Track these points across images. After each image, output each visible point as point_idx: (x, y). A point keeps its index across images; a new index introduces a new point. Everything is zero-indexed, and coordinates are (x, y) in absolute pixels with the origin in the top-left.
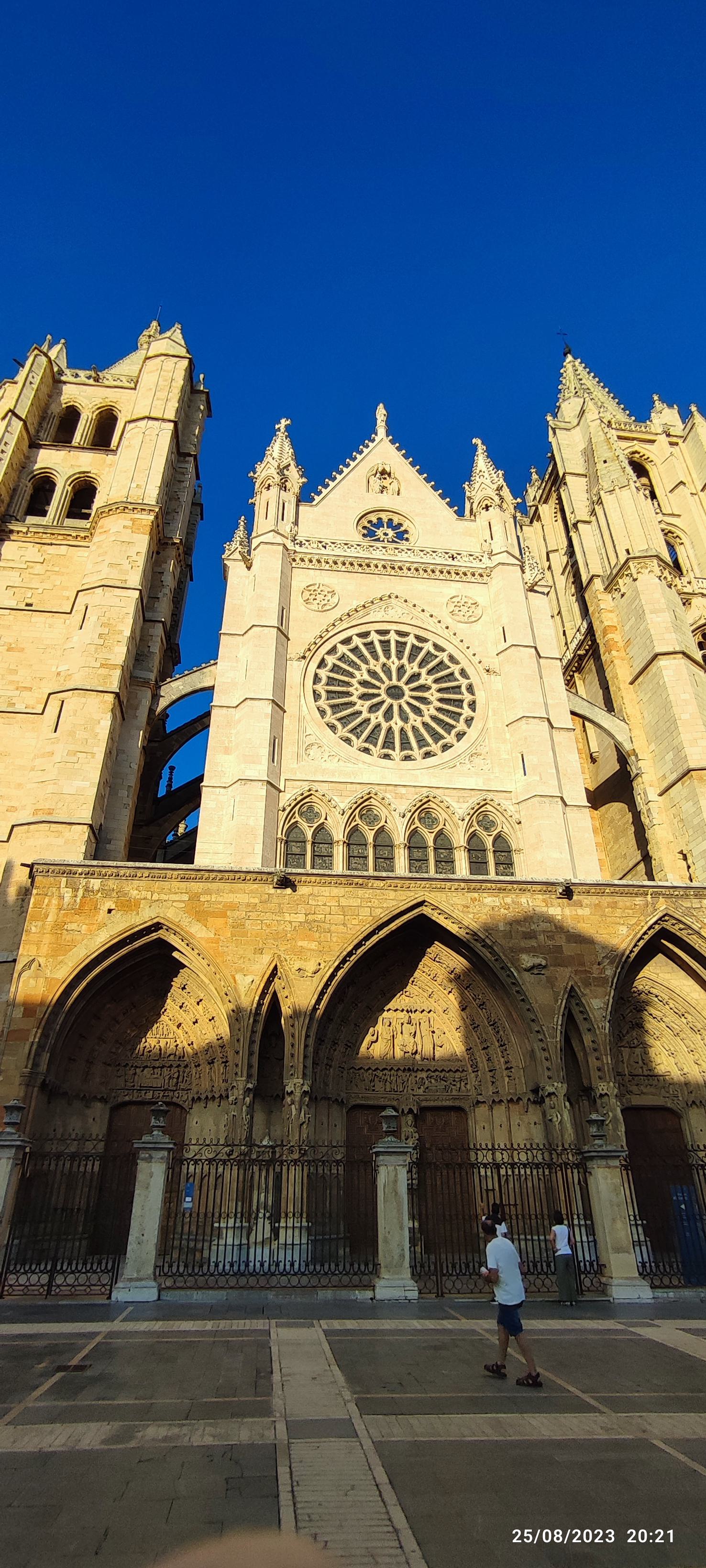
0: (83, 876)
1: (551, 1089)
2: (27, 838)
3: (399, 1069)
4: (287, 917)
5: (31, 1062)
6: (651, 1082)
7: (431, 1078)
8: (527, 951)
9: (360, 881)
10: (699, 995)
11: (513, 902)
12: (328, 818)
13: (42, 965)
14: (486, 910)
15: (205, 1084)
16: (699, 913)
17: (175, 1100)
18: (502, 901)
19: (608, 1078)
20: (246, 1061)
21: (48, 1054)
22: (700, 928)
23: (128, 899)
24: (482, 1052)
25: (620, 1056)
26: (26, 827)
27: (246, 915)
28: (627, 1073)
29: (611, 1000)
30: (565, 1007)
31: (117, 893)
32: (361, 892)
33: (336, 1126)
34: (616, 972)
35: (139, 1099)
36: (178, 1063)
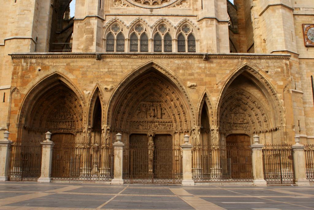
1: (194, 128)
3: (148, 122)
4: (101, 70)
6: (241, 126)
8: (189, 80)
9: (128, 56)
11: (186, 62)
12: (123, 30)
15: (80, 127)
17: (71, 132)
19: (214, 124)
20: (88, 120)
21: (24, 118)
22: (259, 71)
24: (178, 116)
25: (230, 117)
26: (9, 40)
28: (232, 123)
29: (220, 97)
30: (202, 100)
31: (41, 64)
32: (128, 60)
33: (125, 140)
34: (223, 88)
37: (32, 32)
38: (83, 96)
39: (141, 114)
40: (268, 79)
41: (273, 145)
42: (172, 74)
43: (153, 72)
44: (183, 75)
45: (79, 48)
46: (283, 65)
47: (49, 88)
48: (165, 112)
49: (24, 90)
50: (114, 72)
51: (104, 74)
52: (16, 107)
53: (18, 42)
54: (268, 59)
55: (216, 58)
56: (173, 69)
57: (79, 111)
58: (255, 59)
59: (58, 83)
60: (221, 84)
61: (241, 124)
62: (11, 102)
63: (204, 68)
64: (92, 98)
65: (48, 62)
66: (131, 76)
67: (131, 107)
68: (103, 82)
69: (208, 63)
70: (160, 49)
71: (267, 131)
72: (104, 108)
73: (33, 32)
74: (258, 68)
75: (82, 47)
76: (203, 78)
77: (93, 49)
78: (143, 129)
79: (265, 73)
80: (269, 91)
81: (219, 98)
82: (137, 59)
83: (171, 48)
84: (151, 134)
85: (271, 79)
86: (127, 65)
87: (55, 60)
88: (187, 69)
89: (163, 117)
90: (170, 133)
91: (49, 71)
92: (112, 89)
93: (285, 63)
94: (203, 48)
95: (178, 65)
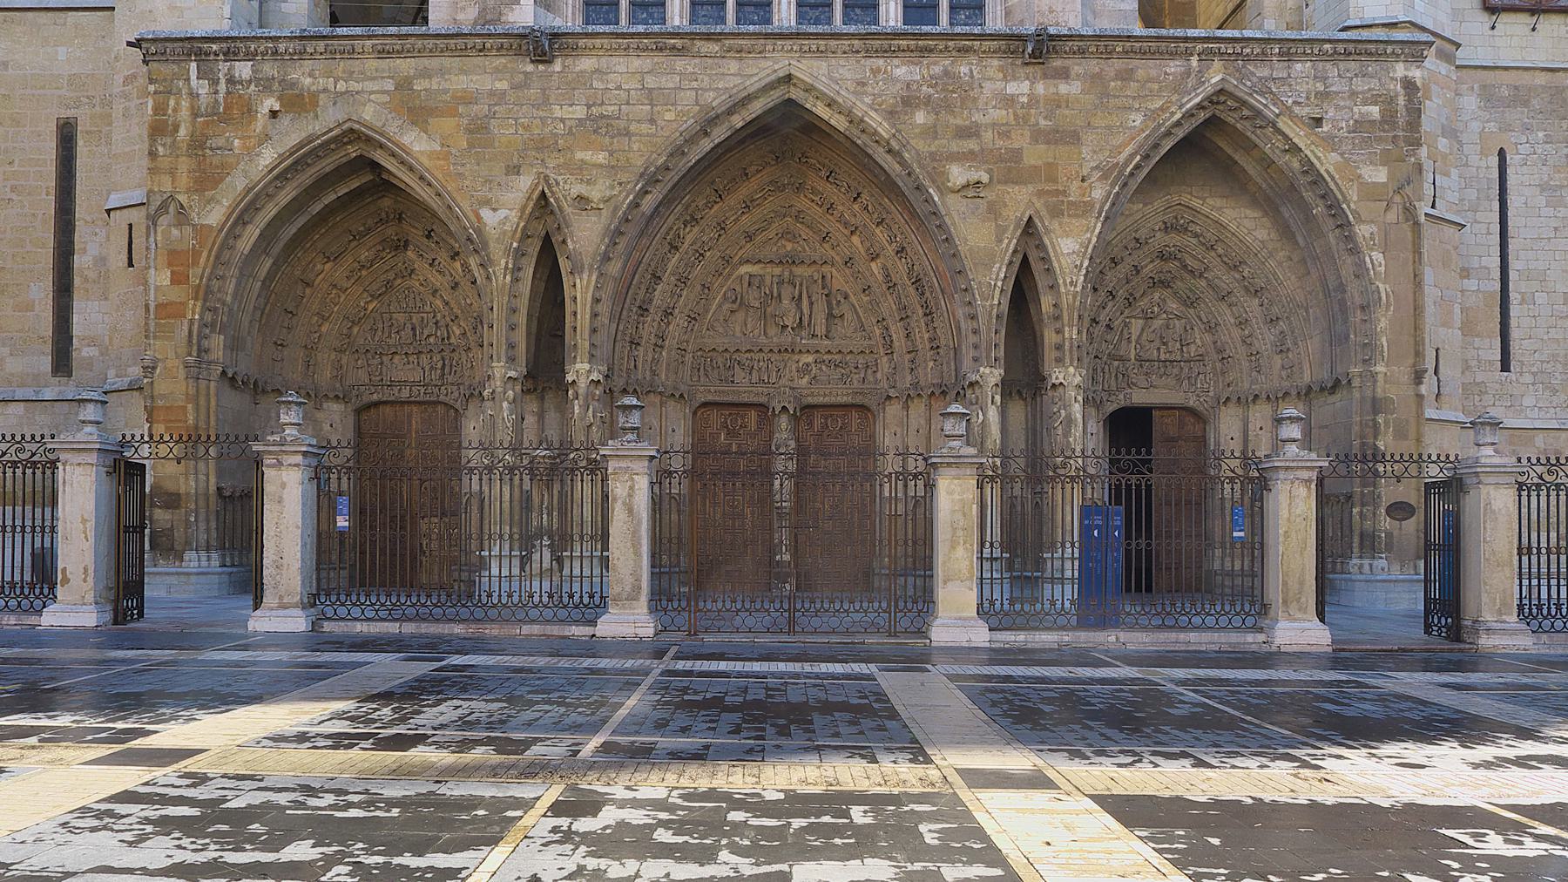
0: (221, 57)
1: (973, 378)
4: (558, 112)
5: (195, 348)
9: (678, 42)
10: (1269, 234)
11: (946, 73)
17: (442, 398)
22: (1277, 116)
27: (489, 110)
29: (1094, 239)
30: (1015, 251)
32: (680, 63)
38: (479, 232)
39: (740, 316)
44: (931, 132)
46: (1392, 87)
48: (845, 308)
51: (570, 133)
54: (1324, 57)
58: (1263, 57)
60: (1100, 179)
63: (1025, 99)
64: (520, 241)
65: (310, 75)
66: (691, 140)
67: (699, 287)
69: (1045, 76)
76: (1021, 149)
79: (1309, 126)
80: (1319, 210)
82: (720, 61)
86: (675, 89)
88: (949, 108)
89: (839, 329)
90: (866, 401)
91: (317, 116)
93: (1406, 77)
95: (908, 85)
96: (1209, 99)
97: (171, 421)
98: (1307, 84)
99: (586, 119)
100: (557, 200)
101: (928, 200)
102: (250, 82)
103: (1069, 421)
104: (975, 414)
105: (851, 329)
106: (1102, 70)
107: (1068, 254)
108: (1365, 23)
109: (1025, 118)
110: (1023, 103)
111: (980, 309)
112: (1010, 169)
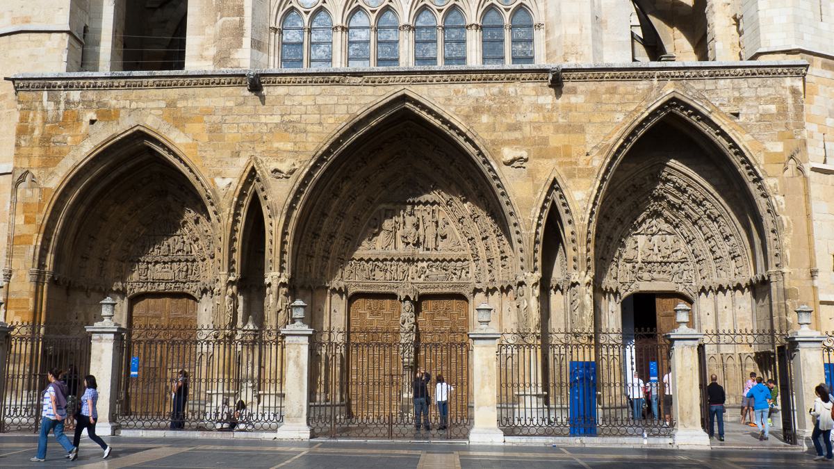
0: (62, 88)
1: (521, 279)
2: (10, 49)
3: (399, 260)
4: (263, 119)
7: (431, 266)
9: (337, 78)
11: (500, 92)
13: (36, 176)
14: (470, 102)
15: (210, 276)
16: (712, 96)
17: (185, 290)
18: (488, 92)
20: (226, 258)
22: (710, 113)
23: (107, 109)
26: (7, 37)
28: (639, 260)
29: (595, 192)
30: (546, 200)
31: (97, 103)
32: (337, 89)
34: (604, 163)
35: (153, 290)
36: (186, 257)
37: (71, 12)
38: (214, 192)
40: (738, 135)
41: (718, 331)
42: (460, 127)
43: (412, 120)
44: (492, 128)
45: (205, 54)
46: (783, 93)
47: (123, 169)
48: (446, 231)
49: (50, 178)
50: (298, 125)
51: (271, 131)
52: (28, 226)
53: (33, 41)
54: (736, 76)
55: (585, 78)
56: (462, 113)
57: (207, 231)
59: (146, 156)
60: (597, 154)
61: (665, 263)
62: (13, 212)
63: (550, 107)
65: (115, 99)
66: (346, 135)
67: (352, 219)
68: (268, 151)
70: (431, 54)
71: (721, 288)
72: (271, 224)
73: (72, 12)
74: (708, 102)
75: (212, 51)
77: (244, 60)
78: (385, 278)
79: (730, 118)
80: (742, 169)
81: (592, 192)
82: (362, 87)
83: (465, 49)
84: (408, 294)
85: (748, 137)
87: (135, 91)
92: (292, 172)
94: (553, 47)
95: (477, 100)
96: (667, 103)
97: (19, 308)
98: (728, 92)
99: (280, 123)
100: (262, 172)
101: (491, 169)
102: (79, 103)
103: (583, 306)
104: (522, 302)
105: (452, 244)
106: (597, 88)
107: (579, 201)
108: (769, 51)
109: (550, 119)
110: (548, 109)
111: (524, 236)
112: (543, 150)
